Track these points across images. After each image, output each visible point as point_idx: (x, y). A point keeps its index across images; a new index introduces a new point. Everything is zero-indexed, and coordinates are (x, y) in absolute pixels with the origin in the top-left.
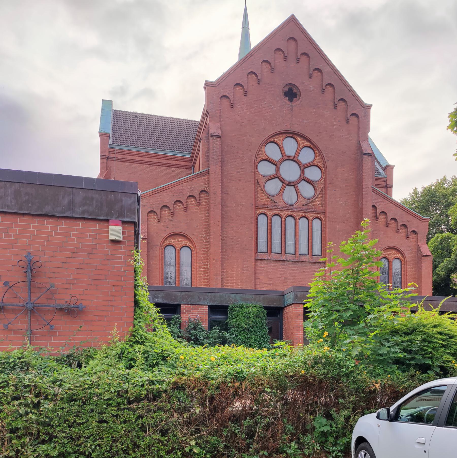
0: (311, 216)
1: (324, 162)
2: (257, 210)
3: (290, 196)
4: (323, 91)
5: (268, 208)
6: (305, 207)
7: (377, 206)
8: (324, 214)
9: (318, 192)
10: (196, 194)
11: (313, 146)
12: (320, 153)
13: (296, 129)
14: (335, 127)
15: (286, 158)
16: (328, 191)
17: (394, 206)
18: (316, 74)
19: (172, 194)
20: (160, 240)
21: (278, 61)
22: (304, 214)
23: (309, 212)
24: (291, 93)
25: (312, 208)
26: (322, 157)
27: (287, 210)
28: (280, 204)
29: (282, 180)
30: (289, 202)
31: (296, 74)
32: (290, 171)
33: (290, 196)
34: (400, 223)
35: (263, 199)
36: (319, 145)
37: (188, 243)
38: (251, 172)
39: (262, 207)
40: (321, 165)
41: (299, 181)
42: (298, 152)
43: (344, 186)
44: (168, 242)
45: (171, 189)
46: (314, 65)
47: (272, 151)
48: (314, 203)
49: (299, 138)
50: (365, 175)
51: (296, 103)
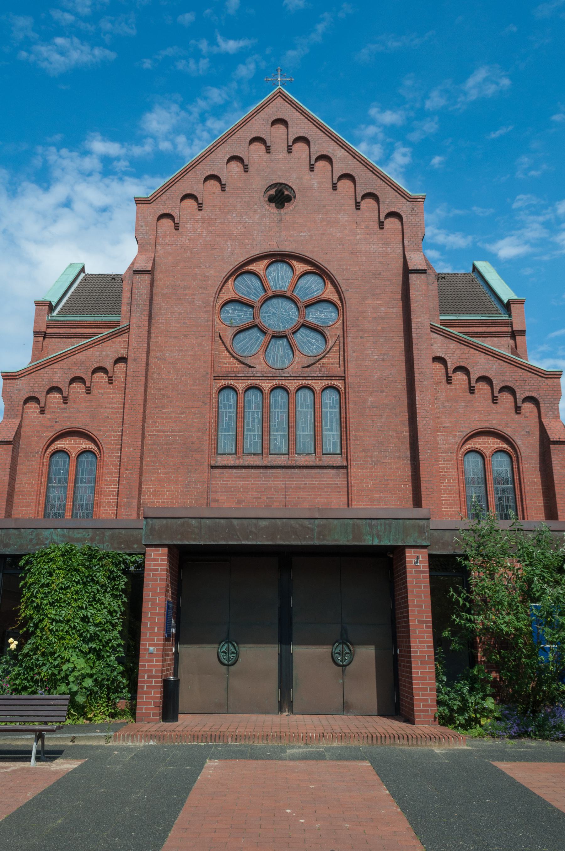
0: (318, 385)
5: (236, 378)
6: (306, 369)
8: (343, 378)
10: (108, 364)
13: (288, 247)
14: (358, 237)
15: (270, 294)
16: (349, 339)
20: (42, 444)
22: (304, 382)
23: (313, 378)
25: (320, 370)
28: (258, 368)
32: (280, 316)
36: (332, 269)
38: (207, 321)
40: (336, 299)
43: (380, 328)
44: (58, 445)
48: (324, 361)
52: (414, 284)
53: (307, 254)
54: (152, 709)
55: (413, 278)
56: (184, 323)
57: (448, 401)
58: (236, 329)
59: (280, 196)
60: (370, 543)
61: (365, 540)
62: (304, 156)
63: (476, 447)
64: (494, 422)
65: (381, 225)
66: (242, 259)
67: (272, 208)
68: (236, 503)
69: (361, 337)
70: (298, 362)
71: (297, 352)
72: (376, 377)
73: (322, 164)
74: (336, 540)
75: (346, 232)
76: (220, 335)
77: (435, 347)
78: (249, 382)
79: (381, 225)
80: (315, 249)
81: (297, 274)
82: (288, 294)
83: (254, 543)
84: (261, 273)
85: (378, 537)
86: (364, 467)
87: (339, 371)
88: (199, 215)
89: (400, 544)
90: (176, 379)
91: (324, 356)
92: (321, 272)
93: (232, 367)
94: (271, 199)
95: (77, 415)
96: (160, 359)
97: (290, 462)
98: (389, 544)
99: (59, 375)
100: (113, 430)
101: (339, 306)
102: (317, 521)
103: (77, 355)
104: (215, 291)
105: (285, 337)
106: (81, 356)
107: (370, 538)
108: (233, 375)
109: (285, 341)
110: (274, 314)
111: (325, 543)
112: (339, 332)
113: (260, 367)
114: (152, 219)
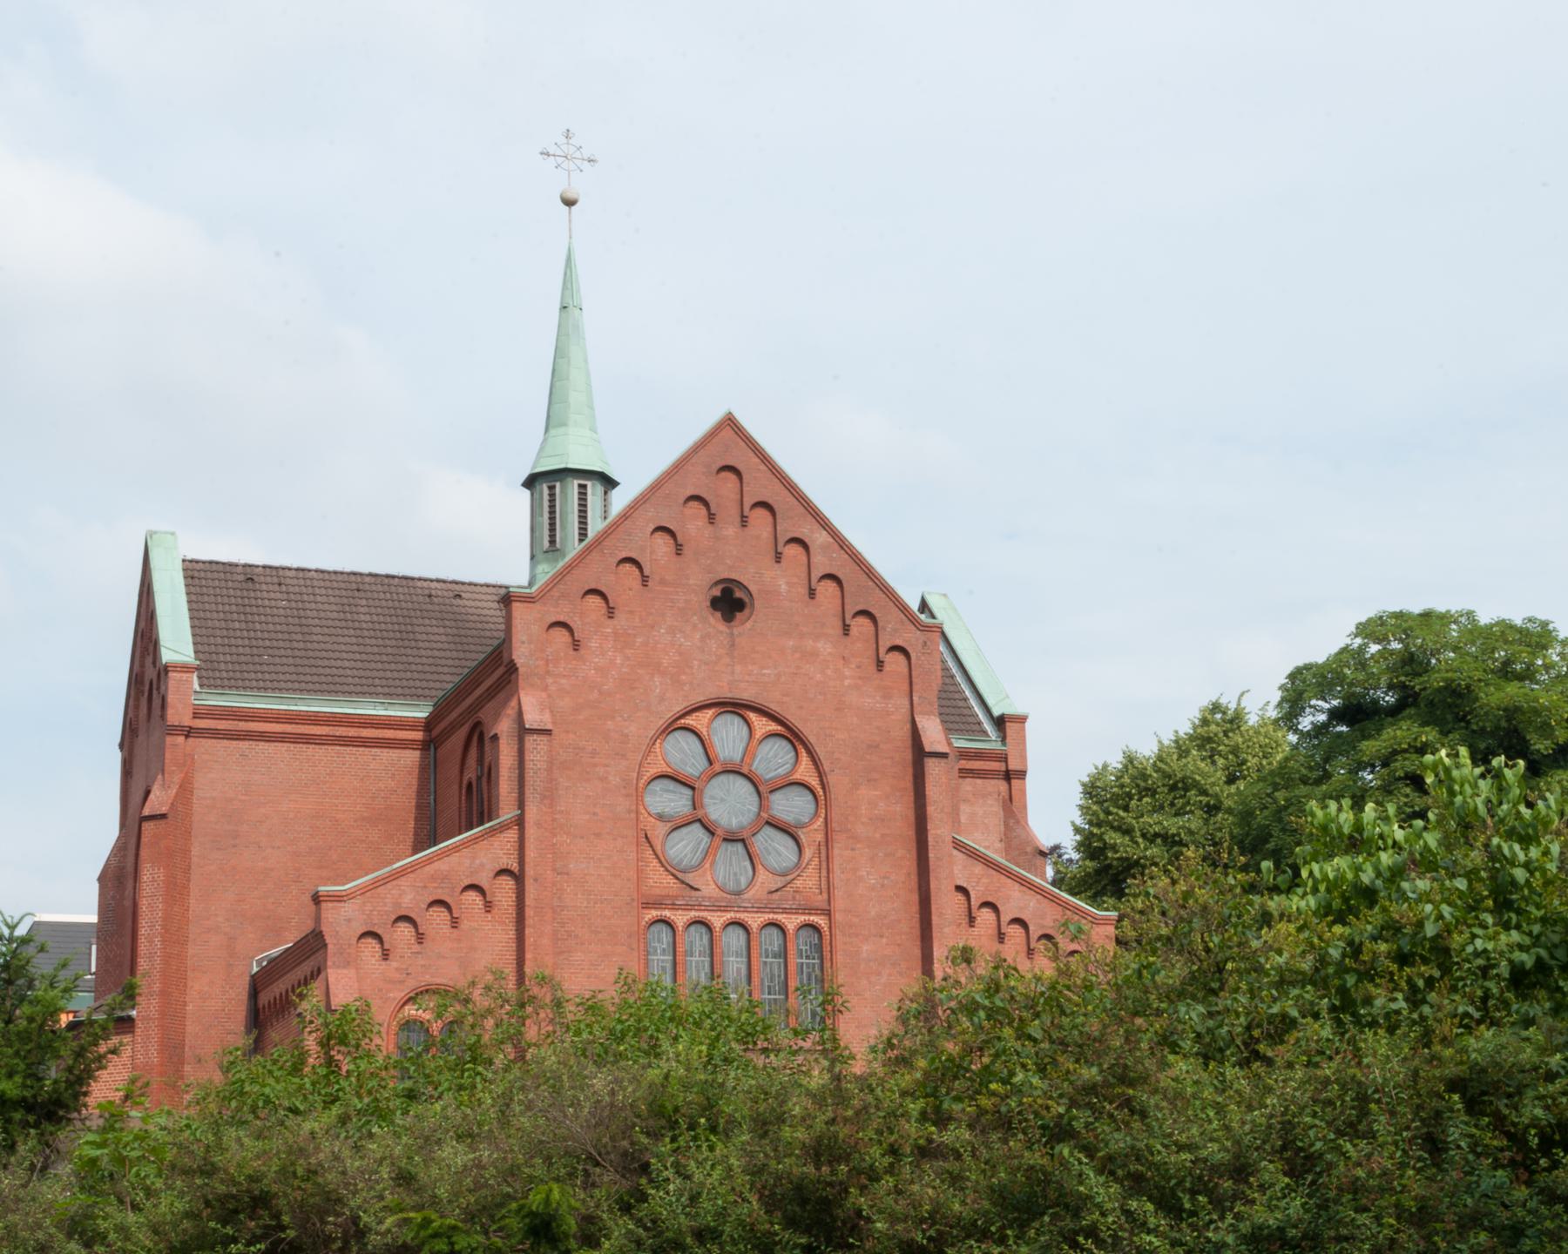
1: (821, 775)
4: (812, 593)
5: (674, 907)
8: (828, 913)
13: (746, 694)
14: (847, 682)
15: (717, 767)
18: (793, 551)
21: (692, 524)
23: (785, 911)
24: (729, 602)
27: (725, 909)
30: (731, 886)
31: (739, 553)
32: (730, 803)
36: (809, 732)
38: (629, 812)
40: (814, 782)
42: (749, 752)
46: (787, 529)
48: (798, 883)
49: (752, 716)
51: (745, 627)
55: (932, 766)
66: (678, 708)
78: (693, 914)
84: (704, 732)
92: (793, 736)
101: (820, 795)
110: (722, 800)
112: (820, 837)
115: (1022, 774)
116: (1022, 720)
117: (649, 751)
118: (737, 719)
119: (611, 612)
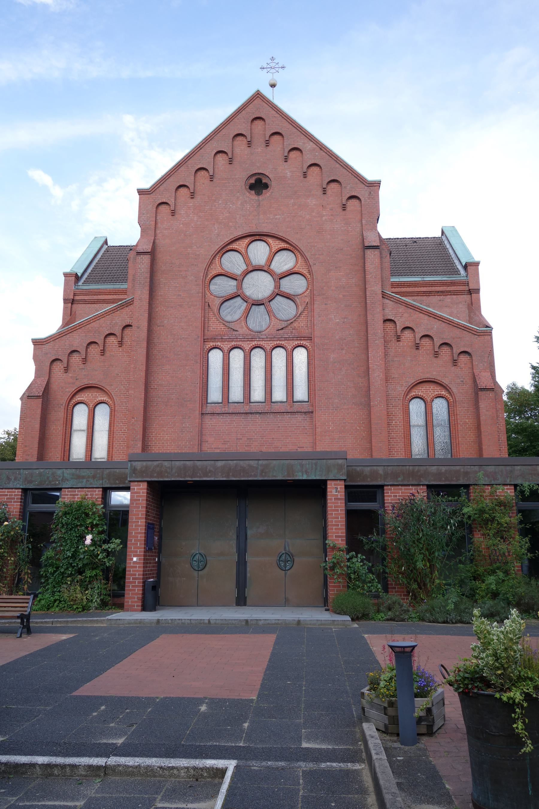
0: (289, 345)
1: (309, 266)
2: (206, 343)
3: (259, 320)
5: (222, 340)
6: (280, 331)
7: (396, 320)
8: (310, 339)
9: (301, 309)
10: (117, 330)
11: (290, 247)
12: (303, 255)
13: (265, 229)
16: (315, 306)
17: (426, 317)
19: (84, 334)
23: (286, 339)
25: (292, 332)
26: (306, 260)
28: (241, 331)
29: (245, 299)
30: (257, 329)
33: (259, 320)
34: (438, 342)
35: (215, 327)
37: (105, 398)
39: (213, 339)
40: (305, 272)
41: (271, 298)
43: (342, 296)
45: (83, 328)
47: (233, 262)
48: (295, 325)
49: (270, 240)
50: (369, 276)
51: (267, 194)
52: (369, 258)
53: (281, 234)
54: (135, 602)
56: (179, 295)
57: (397, 357)
58: (222, 299)
59: (258, 185)
60: (301, 478)
61: (296, 476)
62: (279, 149)
63: (420, 394)
64: (434, 373)
65: (344, 207)
66: (227, 240)
67: (252, 196)
68: (222, 444)
69: (325, 304)
70: (273, 325)
71: (272, 317)
72: (337, 337)
73: (294, 154)
74: (275, 476)
75: (314, 214)
76: (209, 305)
77: (387, 311)
78: (233, 343)
79: (344, 207)
80: (288, 230)
81: (273, 251)
82: (265, 269)
83: (213, 479)
85: (306, 474)
86: (326, 412)
87: (306, 332)
88: (191, 203)
89: (324, 478)
90: (173, 342)
91: (295, 321)
93: (218, 331)
94: (252, 187)
95: (93, 373)
96: (160, 326)
97: (266, 409)
98: (315, 478)
99: (78, 340)
100: (122, 385)
102: (260, 462)
103: (92, 324)
104: (205, 267)
105: (263, 304)
106: (95, 325)
107: (300, 474)
108: (220, 338)
109: (262, 307)
111: (266, 478)
112: (307, 300)
113: (243, 330)
114: (152, 208)
115: (477, 291)
116: (477, 264)
117: (211, 263)
118: (263, 244)
119: (192, 195)
